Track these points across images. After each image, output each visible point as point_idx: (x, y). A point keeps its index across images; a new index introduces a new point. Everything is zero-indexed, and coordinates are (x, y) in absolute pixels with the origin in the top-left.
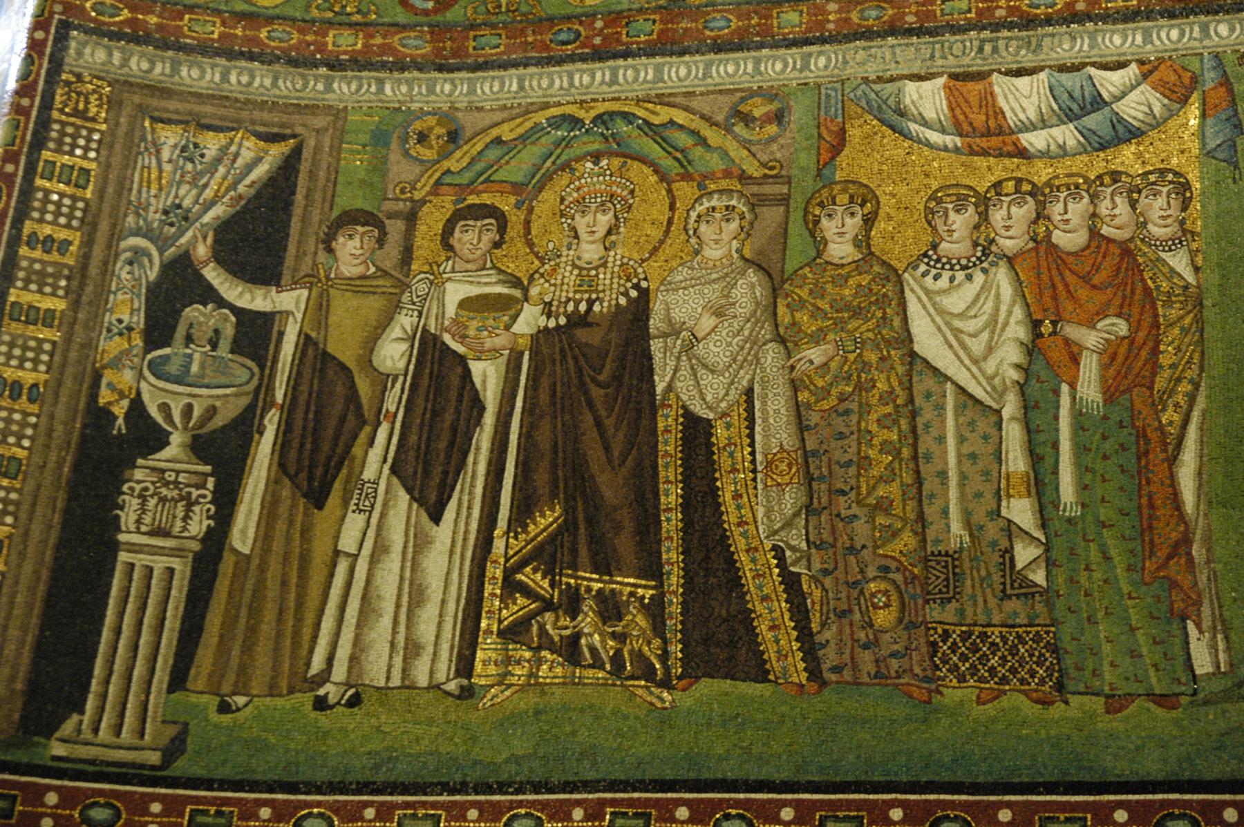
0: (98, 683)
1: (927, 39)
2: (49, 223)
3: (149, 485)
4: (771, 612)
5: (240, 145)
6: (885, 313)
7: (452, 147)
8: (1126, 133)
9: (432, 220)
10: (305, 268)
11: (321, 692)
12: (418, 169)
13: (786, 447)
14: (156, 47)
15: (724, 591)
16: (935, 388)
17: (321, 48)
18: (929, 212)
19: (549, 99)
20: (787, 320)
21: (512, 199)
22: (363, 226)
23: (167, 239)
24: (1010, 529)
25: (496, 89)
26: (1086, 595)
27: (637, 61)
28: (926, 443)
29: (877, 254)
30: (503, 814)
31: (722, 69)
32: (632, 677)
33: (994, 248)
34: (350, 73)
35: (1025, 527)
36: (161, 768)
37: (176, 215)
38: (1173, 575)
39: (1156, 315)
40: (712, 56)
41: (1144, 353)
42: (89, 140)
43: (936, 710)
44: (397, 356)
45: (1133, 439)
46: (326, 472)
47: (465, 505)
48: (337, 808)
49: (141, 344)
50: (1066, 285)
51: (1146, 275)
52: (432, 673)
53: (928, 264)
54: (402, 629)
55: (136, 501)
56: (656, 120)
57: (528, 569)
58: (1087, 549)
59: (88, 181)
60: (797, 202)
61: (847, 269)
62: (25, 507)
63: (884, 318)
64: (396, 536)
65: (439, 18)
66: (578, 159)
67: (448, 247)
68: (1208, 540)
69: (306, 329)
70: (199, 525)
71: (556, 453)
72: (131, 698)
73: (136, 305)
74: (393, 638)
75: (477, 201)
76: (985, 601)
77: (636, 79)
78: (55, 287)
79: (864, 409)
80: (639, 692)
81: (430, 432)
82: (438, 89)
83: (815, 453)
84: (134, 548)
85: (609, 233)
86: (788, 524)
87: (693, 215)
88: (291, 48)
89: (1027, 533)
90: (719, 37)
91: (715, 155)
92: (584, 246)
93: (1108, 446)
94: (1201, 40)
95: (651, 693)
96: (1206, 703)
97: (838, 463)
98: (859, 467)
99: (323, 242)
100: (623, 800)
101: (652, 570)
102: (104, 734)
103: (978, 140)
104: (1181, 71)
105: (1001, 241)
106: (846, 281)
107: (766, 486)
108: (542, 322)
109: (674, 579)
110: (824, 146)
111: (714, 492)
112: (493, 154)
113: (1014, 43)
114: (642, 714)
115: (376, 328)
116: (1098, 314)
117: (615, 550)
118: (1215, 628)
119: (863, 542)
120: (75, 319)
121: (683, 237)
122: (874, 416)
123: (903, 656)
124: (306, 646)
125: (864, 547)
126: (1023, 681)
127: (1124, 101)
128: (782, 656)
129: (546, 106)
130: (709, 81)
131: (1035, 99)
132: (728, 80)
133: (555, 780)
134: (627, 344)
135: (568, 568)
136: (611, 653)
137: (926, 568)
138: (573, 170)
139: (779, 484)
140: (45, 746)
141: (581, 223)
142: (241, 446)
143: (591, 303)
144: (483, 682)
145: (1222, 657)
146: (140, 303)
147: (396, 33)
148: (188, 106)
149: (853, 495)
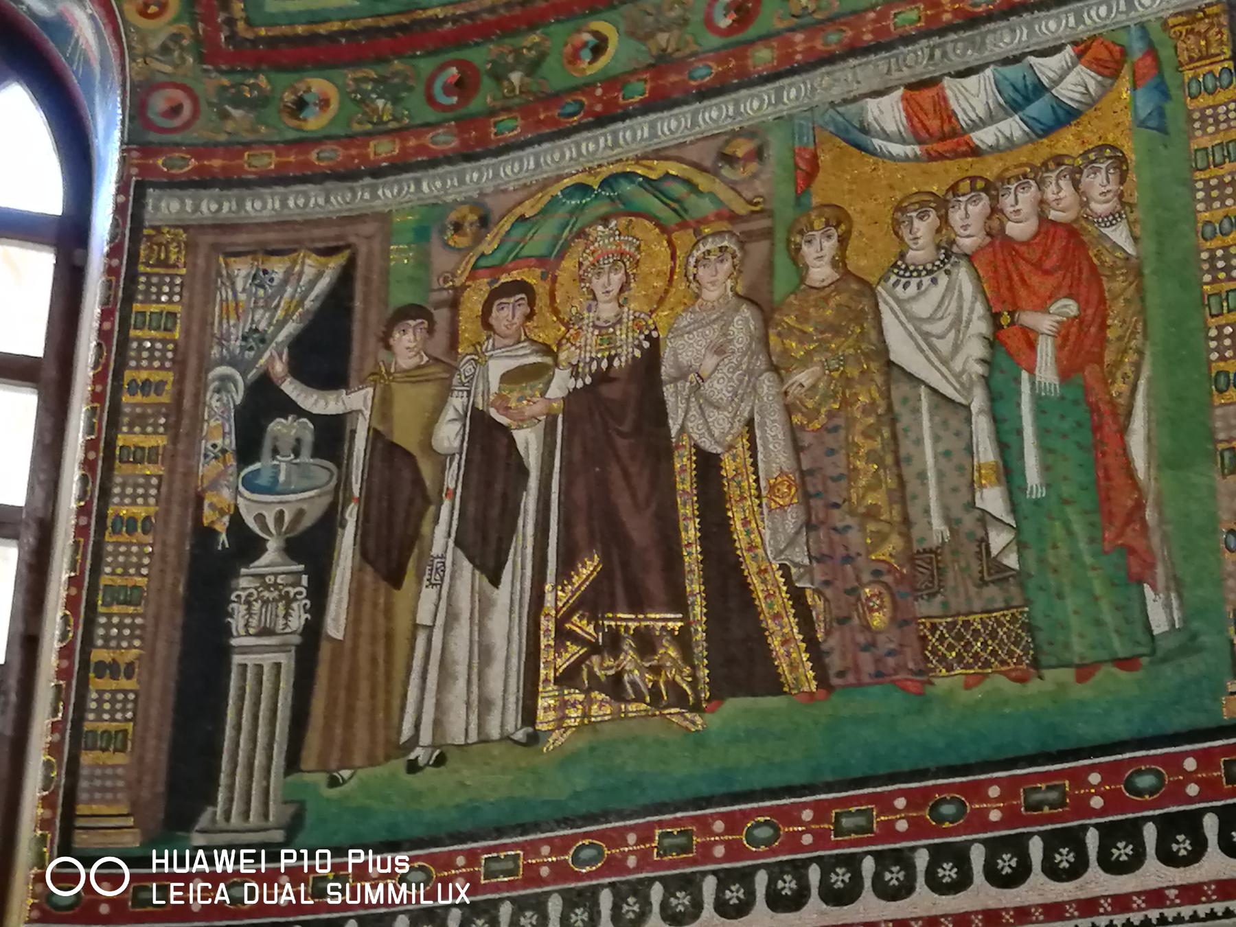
1: (884, 54)
2: (146, 369)
3: (253, 591)
5: (303, 263)
6: (862, 328)
7: (483, 230)
8: (1067, 116)
9: (473, 301)
10: (369, 366)
11: (412, 756)
12: (455, 257)
13: (786, 470)
17: (364, 158)
18: (896, 224)
19: (561, 172)
20: (778, 349)
21: (538, 271)
22: (414, 319)
24: (985, 518)
25: (516, 170)
28: (906, 447)
30: (570, 848)
31: (707, 115)
33: (955, 249)
34: (391, 178)
39: (1102, 291)
40: (697, 105)
41: (1093, 330)
42: (172, 285)
44: (453, 436)
45: (1088, 415)
48: (430, 858)
49: (235, 464)
51: (1091, 254)
52: (502, 726)
53: (897, 274)
54: (475, 689)
55: (243, 608)
56: (653, 176)
57: (575, 618)
59: (175, 323)
60: (780, 235)
64: (464, 604)
67: (487, 326)
68: (1159, 505)
69: (375, 425)
70: (298, 620)
72: (254, 785)
73: (227, 429)
75: (509, 279)
78: (156, 425)
79: (851, 422)
82: (468, 178)
83: (811, 472)
85: (621, 290)
86: (791, 543)
87: (692, 261)
92: (601, 306)
93: (1066, 426)
95: (686, 719)
96: (1165, 660)
101: (679, 603)
103: (935, 145)
104: (1111, 46)
105: (961, 241)
107: (770, 510)
108: (571, 386)
109: (698, 609)
110: (801, 174)
112: (517, 234)
113: (960, 45)
116: (1050, 298)
122: (859, 427)
126: (1003, 663)
128: (793, 667)
129: (559, 178)
130: (697, 129)
131: (983, 95)
132: (713, 125)
136: (650, 685)
137: (914, 566)
138: (586, 236)
141: (598, 284)
143: (611, 359)
145: (1176, 615)
146: (230, 426)
149: (845, 506)
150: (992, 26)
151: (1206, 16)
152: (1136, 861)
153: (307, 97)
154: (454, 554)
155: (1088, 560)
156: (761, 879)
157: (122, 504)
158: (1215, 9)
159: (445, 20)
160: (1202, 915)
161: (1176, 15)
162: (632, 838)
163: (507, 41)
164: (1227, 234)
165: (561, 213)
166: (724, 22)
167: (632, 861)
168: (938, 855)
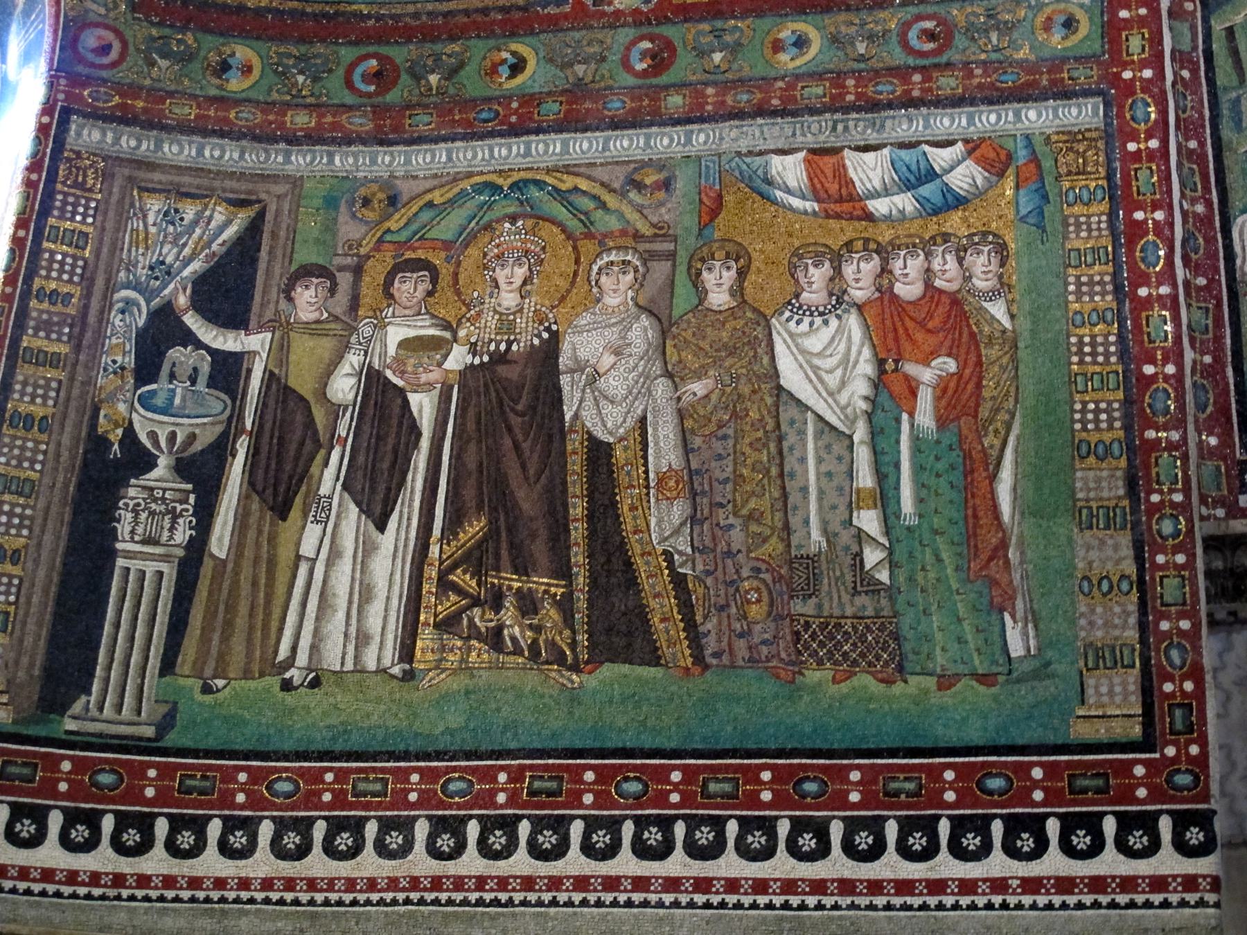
0: (102, 669)
1: (790, 119)
3: (141, 501)
4: (662, 606)
5: (213, 210)
6: (756, 352)
7: (391, 209)
8: (954, 202)
9: (376, 271)
10: (269, 314)
11: (287, 675)
12: (364, 229)
14: (142, 128)
15: (623, 588)
16: (797, 416)
20: (675, 358)
21: (443, 254)
23: (152, 291)
24: (860, 536)
25: (428, 160)
26: (922, 591)
27: (547, 137)
28: (791, 463)
29: (750, 302)
30: (440, 777)
32: (547, 663)
33: (846, 298)
34: (305, 148)
35: (873, 535)
36: (156, 740)
37: (160, 271)
38: (993, 573)
39: (979, 356)
40: (610, 133)
41: (970, 387)
42: (87, 207)
43: (799, 689)
44: (347, 389)
45: (960, 460)
46: (289, 489)
47: (406, 516)
50: (906, 330)
51: (971, 322)
52: (379, 659)
53: (791, 311)
54: (354, 621)
55: (130, 515)
56: (563, 187)
58: (923, 552)
59: (87, 243)
60: (682, 257)
61: (726, 314)
62: (39, 521)
63: (755, 356)
64: (348, 543)
65: (380, 99)
66: (498, 221)
69: (270, 367)
70: (182, 534)
71: (481, 472)
72: (129, 681)
73: (128, 348)
74: (347, 630)
76: (840, 597)
77: (546, 152)
78: (60, 334)
80: (553, 674)
81: (376, 453)
83: (698, 472)
84: (129, 555)
85: (525, 283)
87: (595, 268)
88: (256, 126)
89: (874, 539)
90: (615, 116)
91: (613, 217)
92: (503, 294)
94: (1015, 123)
95: (562, 676)
96: (1018, 681)
97: (717, 480)
98: (735, 484)
99: (284, 291)
100: (540, 765)
101: (563, 571)
102: (108, 711)
103: (832, 206)
105: (852, 292)
106: (724, 325)
107: (657, 500)
108: (469, 359)
111: (614, 504)
112: (426, 216)
113: (861, 124)
114: (555, 693)
115: (329, 365)
116: (932, 353)
117: (532, 555)
118: (1026, 618)
119: (739, 547)
120: (77, 361)
121: (586, 287)
122: (747, 441)
123: (772, 644)
124: (273, 636)
125: (739, 551)
127: (952, 174)
130: (607, 153)
131: (879, 170)
132: (623, 153)
133: (483, 748)
134: (540, 378)
135: (493, 570)
137: (791, 569)
139: (668, 499)
140: (60, 722)
141: (501, 275)
142: (217, 467)
143: (509, 343)
144: (422, 667)
145: (1032, 643)
146: (130, 346)
147: (344, 113)
148: (170, 178)
149: (730, 506)
150: (892, 113)
151: (1084, 139)
152: (985, 850)
153: (230, 61)
154: (341, 496)
155: (955, 586)
156: (628, 829)
157: (21, 400)
158: (1094, 135)
159: (369, 16)
160: (1041, 905)
161: (1058, 133)
162: (502, 777)
163: (428, 45)
164: (1095, 325)
165: (471, 206)
166: (640, 66)
167: (501, 798)
168: (799, 826)
